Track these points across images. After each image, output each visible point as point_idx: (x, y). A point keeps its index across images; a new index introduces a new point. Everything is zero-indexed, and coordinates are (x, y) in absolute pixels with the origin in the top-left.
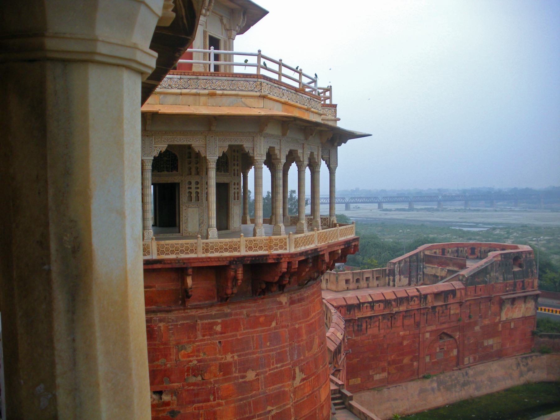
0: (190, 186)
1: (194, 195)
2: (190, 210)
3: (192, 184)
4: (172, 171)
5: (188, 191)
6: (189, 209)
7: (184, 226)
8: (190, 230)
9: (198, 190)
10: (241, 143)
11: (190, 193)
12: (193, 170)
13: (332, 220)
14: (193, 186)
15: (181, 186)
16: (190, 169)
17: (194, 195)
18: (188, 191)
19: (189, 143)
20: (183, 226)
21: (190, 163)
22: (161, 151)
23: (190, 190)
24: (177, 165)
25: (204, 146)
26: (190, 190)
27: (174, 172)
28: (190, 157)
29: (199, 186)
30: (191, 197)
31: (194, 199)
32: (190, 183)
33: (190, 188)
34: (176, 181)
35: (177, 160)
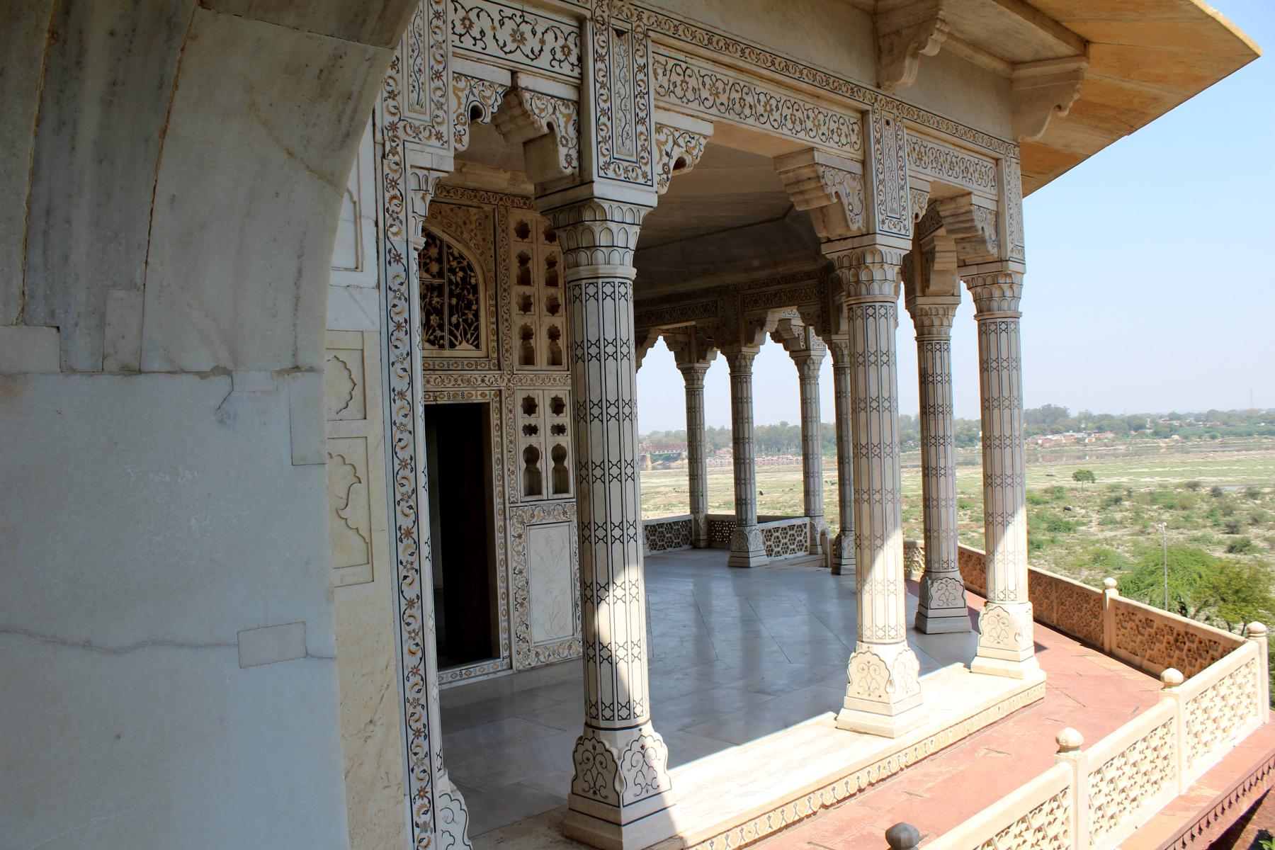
0: (532, 420)
1: (546, 465)
2: (537, 536)
3: (540, 409)
4: (452, 346)
5: (524, 441)
6: (534, 532)
7: (515, 616)
8: (538, 634)
9: (566, 441)
10: (968, 186)
11: (532, 455)
12: (541, 344)
13: (819, 529)
14: (544, 418)
15: (494, 419)
16: (527, 335)
17: (546, 465)
18: (524, 441)
19: (803, 139)
20: (507, 626)
21: (526, 306)
22: (680, 164)
23: (533, 440)
24: (476, 315)
25: (857, 168)
26: (533, 440)
27: (464, 350)
28: (525, 279)
29: (565, 419)
30: (538, 473)
31: (547, 483)
32: (530, 406)
33: (531, 430)
34: (477, 399)
35: (475, 289)
